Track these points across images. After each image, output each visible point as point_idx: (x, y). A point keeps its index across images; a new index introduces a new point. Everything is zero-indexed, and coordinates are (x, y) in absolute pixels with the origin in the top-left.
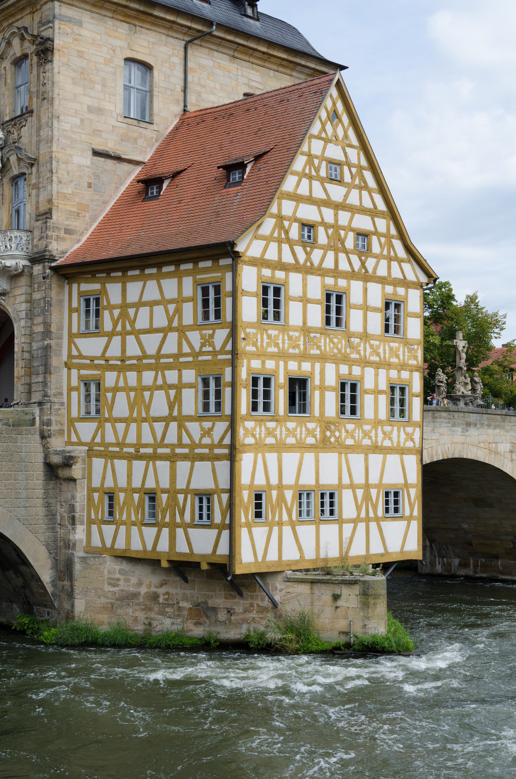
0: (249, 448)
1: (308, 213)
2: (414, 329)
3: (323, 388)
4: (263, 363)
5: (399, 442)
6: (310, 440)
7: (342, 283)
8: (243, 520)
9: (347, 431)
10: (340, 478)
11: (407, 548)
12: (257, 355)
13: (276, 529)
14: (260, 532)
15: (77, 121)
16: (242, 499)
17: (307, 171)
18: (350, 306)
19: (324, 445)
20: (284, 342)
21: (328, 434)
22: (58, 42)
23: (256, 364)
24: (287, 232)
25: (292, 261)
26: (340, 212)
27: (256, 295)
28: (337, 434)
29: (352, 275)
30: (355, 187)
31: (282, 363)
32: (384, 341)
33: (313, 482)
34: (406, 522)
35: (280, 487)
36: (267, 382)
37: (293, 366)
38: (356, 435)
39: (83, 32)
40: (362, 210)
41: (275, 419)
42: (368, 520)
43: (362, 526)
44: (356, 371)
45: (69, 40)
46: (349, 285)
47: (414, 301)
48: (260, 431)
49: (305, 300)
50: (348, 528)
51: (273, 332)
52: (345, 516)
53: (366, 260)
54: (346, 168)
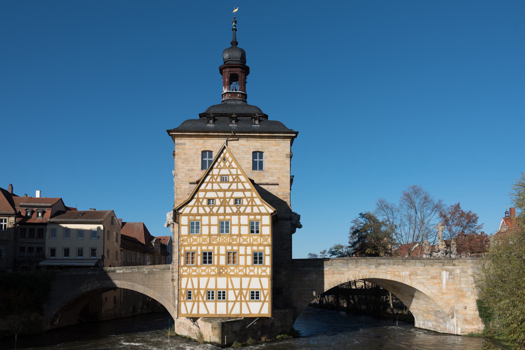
0: (185, 276)
1: (210, 195)
2: (266, 231)
3: (219, 255)
4: (191, 248)
5: (258, 273)
6: (213, 273)
7: (228, 217)
8: (182, 299)
9: (230, 269)
10: (227, 286)
11: (262, 312)
12: (188, 245)
13: (196, 303)
14: (189, 304)
15: (184, 175)
16: (182, 292)
17: (211, 181)
18: (232, 225)
19: (220, 274)
20: (200, 240)
21: (221, 271)
22: (176, 152)
23: (188, 248)
24: (201, 203)
25: (204, 212)
26: (227, 193)
27: (188, 225)
28: (226, 271)
29: (233, 214)
30: (235, 182)
31: (199, 248)
32: (250, 236)
33: (214, 287)
34: (261, 303)
35: (199, 289)
36: (193, 254)
37: (204, 248)
38: (235, 271)
39: (186, 146)
40: (238, 190)
41: (197, 266)
42: (241, 301)
43: (238, 304)
44: (235, 248)
45: (181, 150)
46: (231, 218)
47: (267, 220)
48: (190, 271)
49: (210, 225)
50: (230, 305)
51: (195, 237)
52: (229, 300)
53: (240, 208)
54: (230, 177)
